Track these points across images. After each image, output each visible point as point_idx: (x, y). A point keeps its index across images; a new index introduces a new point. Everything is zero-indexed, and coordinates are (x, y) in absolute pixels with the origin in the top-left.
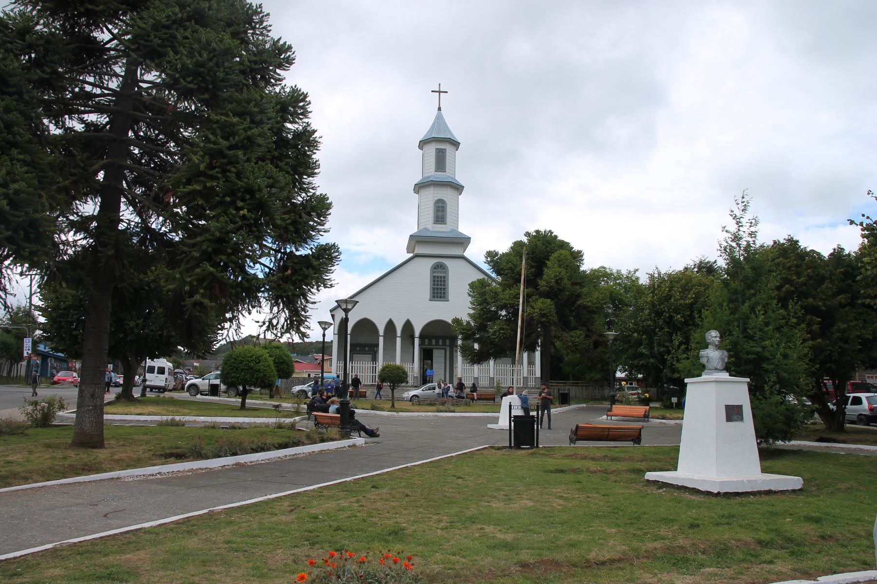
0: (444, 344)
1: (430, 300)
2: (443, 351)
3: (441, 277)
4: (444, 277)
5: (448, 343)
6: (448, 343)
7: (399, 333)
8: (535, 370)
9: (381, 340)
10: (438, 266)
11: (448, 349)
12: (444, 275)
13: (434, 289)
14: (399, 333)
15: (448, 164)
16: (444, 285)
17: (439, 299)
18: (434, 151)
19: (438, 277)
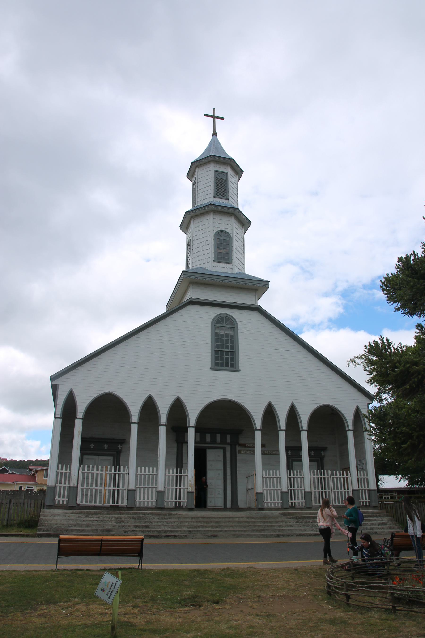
0: (224, 441)
1: (212, 369)
2: (221, 452)
3: (227, 336)
4: (232, 336)
5: (229, 440)
6: (229, 440)
7: (163, 419)
8: (367, 479)
9: (134, 429)
10: (222, 319)
11: (228, 448)
12: (231, 333)
13: (217, 352)
14: (163, 419)
15: (230, 192)
16: (232, 347)
17: (224, 368)
18: (212, 173)
19: (222, 335)
